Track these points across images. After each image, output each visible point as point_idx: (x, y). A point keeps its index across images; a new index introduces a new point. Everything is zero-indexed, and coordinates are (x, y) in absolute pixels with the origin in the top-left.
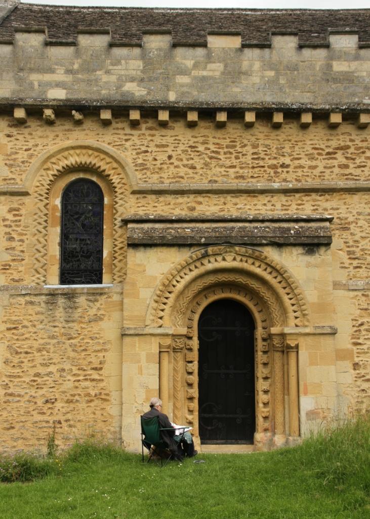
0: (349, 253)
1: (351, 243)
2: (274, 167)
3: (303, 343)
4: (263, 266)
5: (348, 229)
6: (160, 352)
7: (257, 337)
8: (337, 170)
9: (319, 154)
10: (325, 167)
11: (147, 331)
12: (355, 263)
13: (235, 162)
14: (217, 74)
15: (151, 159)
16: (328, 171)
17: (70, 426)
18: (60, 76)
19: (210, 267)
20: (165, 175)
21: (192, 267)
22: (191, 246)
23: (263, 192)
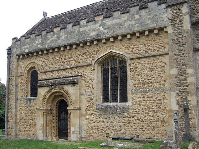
0: (86, 85)
1: (87, 82)
2: (69, 61)
3: (72, 112)
5: (86, 77)
6: (44, 114)
8: (83, 60)
9: (79, 56)
10: (81, 60)
11: (41, 109)
12: (87, 87)
13: (61, 61)
14: (55, 38)
15: (44, 63)
16: (81, 61)
17: (30, 132)
18: (27, 46)
19: (53, 91)
20: (47, 67)
21: (50, 92)
22: (49, 86)
23: (66, 69)
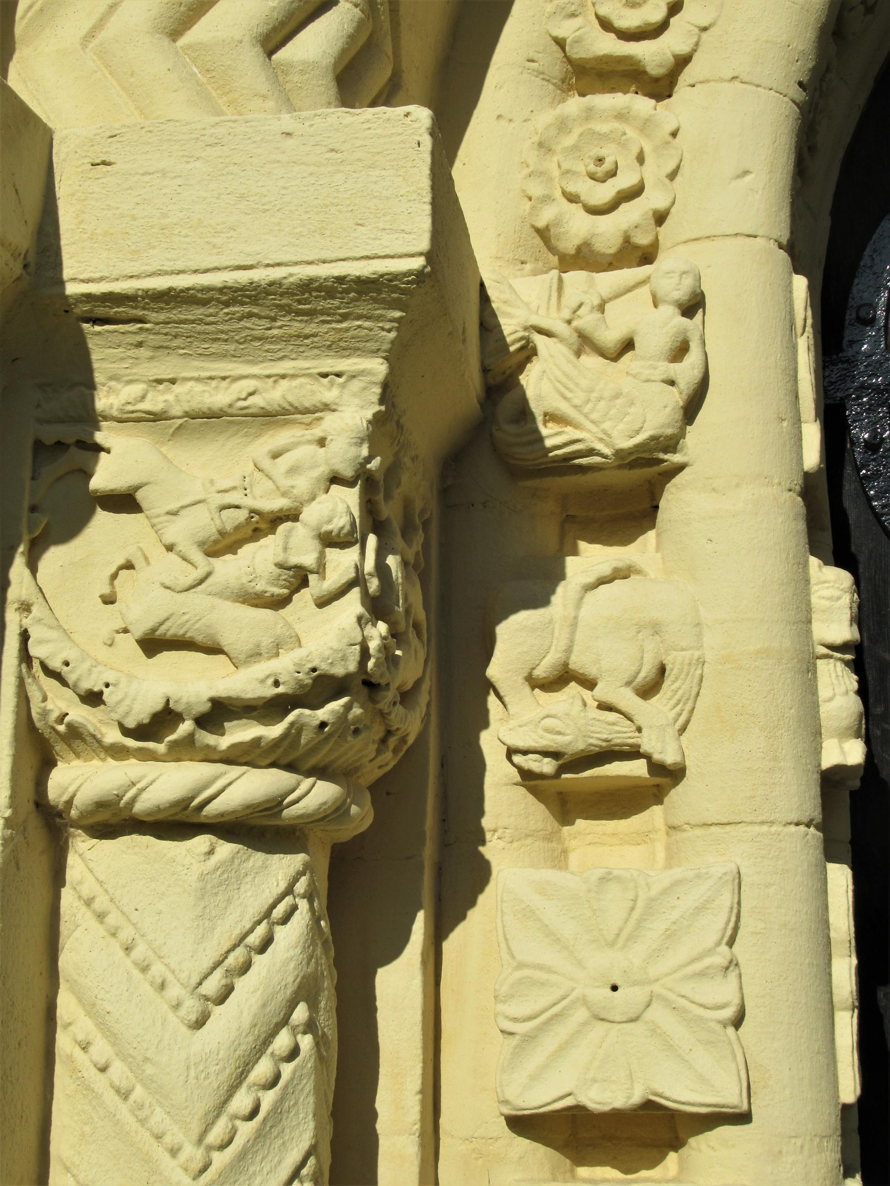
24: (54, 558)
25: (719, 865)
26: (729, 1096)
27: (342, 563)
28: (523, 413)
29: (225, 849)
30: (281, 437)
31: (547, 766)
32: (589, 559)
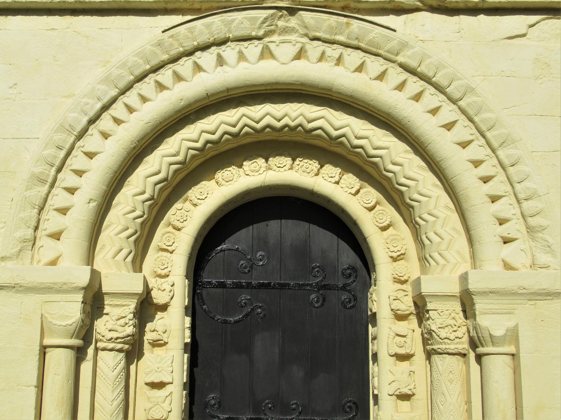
4: (396, 75)
6: (44, 350)
7: (374, 307)
24: (99, 320)
25: (171, 354)
26: (170, 381)
27: (131, 322)
28: (151, 297)
29: (116, 353)
30: (125, 308)
31: (152, 341)
32: (159, 315)
